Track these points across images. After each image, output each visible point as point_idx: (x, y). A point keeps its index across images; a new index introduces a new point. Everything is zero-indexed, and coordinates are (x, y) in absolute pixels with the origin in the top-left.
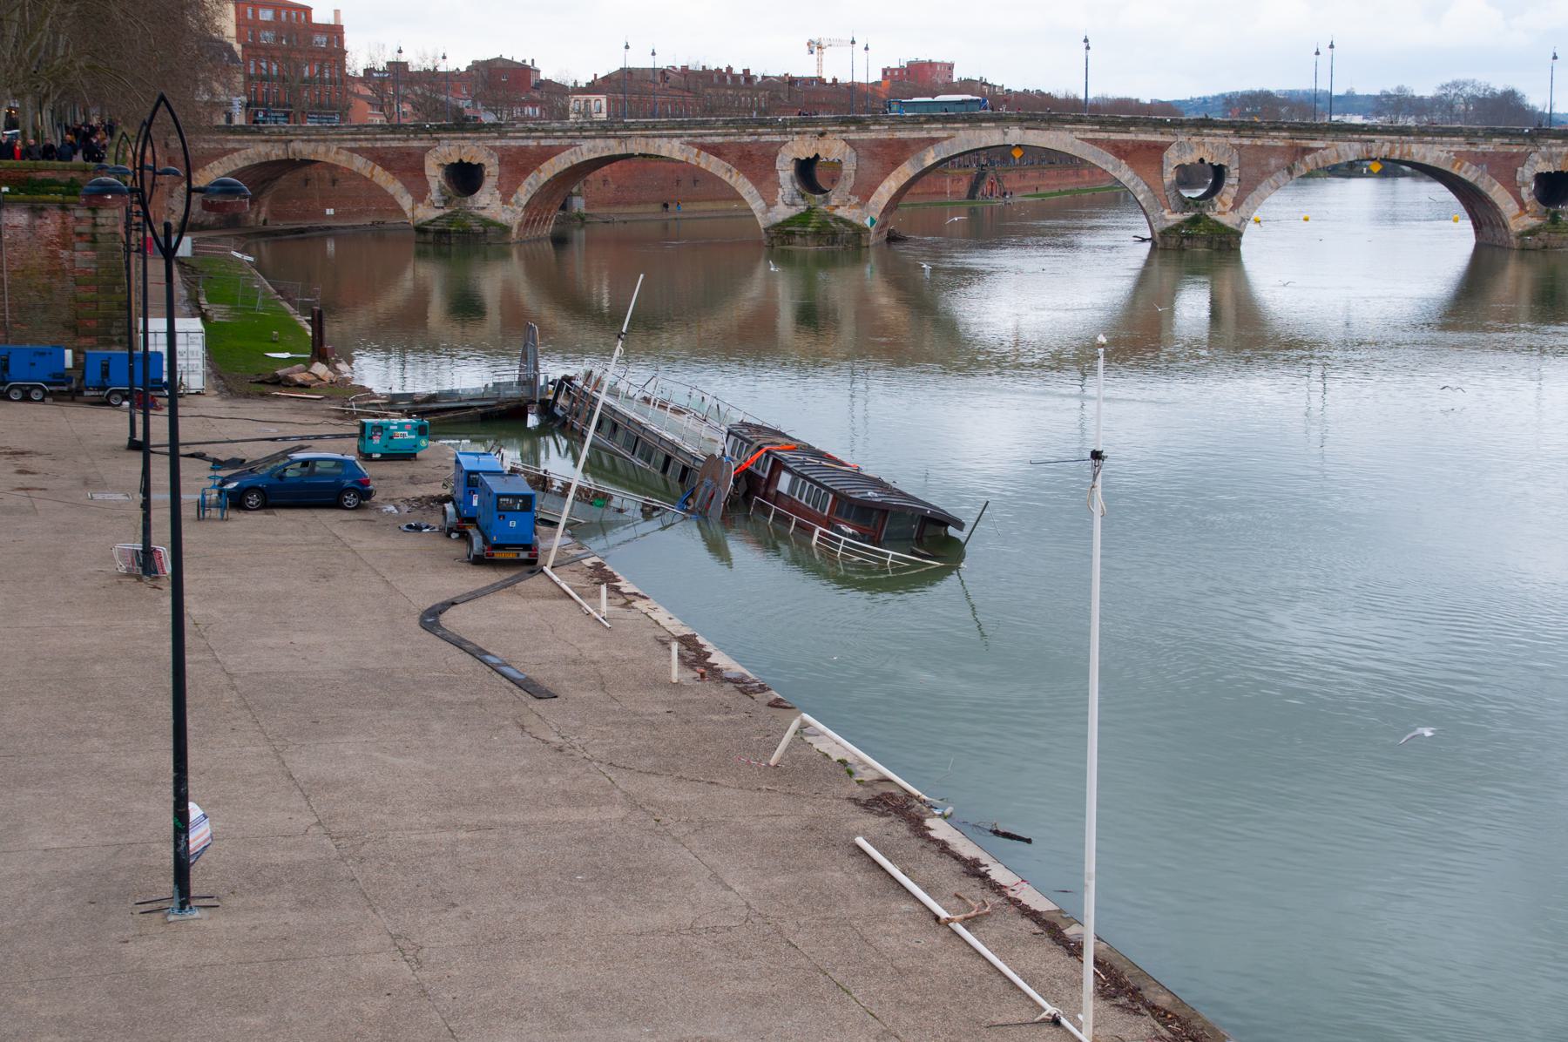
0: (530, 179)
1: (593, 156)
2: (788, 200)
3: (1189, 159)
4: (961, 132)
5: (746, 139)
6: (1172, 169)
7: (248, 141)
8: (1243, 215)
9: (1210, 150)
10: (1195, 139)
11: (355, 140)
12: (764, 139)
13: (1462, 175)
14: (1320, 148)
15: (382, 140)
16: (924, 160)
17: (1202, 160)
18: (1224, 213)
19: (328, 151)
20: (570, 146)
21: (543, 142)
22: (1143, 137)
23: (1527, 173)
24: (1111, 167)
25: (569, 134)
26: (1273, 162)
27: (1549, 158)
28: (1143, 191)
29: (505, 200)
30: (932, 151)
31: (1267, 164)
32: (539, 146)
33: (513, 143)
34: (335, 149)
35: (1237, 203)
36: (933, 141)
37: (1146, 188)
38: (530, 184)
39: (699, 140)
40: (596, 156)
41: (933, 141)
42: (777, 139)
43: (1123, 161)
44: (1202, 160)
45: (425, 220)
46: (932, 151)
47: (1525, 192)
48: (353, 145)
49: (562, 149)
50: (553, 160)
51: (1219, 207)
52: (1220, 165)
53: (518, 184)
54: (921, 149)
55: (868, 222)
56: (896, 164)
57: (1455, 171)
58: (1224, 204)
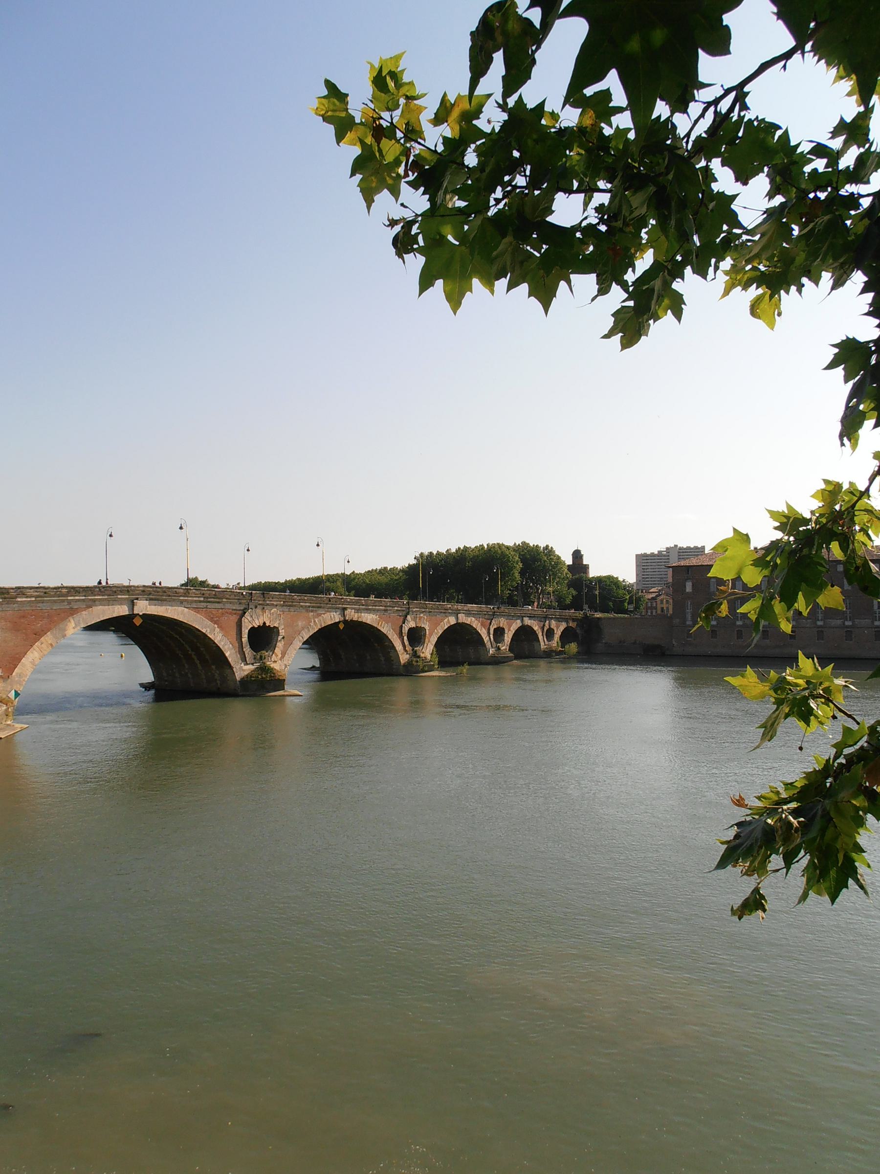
3: (257, 623)
6: (247, 631)
8: (285, 662)
9: (269, 616)
13: (382, 630)
14: (322, 614)
16: (65, 630)
17: (264, 623)
18: (275, 662)
23: (406, 629)
24: (208, 631)
26: (300, 624)
27: (415, 619)
28: (229, 648)
30: (72, 621)
31: (298, 625)
35: (284, 654)
36: (72, 612)
37: (231, 646)
43: (216, 626)
44: (264, 623)
46: (72, 621)
47: (405, 638)
51: (274, 658)
52: (274, 627)
54: (63, 619)
55: (12, 695)
56: (38, 635)
57: (380, 628)
58: (277, 656)
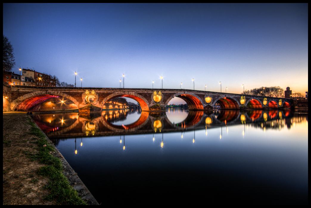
0: (105, 99)
1: (118, 95)
2: (153, 103)
4: (179, 92)
5: (146, 92)
7: (36, 90)
10: (208, 94)
11: (65, 90)
12: (149, 92)
15: (72, 90)
19: (58, 93)
20: (113, 93)
21: (108, 92)
22: (202, 94)
25: (114, 90)
29: (100, 103)
32: (107, 93)
33: (102, 92)
34: (59, 92)
38: (105, 100)
39: (138, 92)
40: (119, 95)
41: (175, 93)
42: (151, 92)
45: (82, 107)
48: (64, 91)
49: (112, 93)
50: (110, 95)
53: (103, 100)
